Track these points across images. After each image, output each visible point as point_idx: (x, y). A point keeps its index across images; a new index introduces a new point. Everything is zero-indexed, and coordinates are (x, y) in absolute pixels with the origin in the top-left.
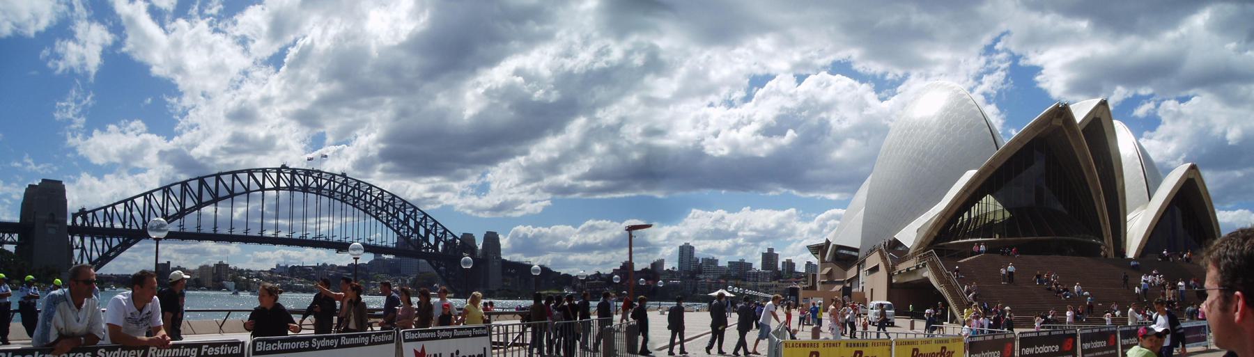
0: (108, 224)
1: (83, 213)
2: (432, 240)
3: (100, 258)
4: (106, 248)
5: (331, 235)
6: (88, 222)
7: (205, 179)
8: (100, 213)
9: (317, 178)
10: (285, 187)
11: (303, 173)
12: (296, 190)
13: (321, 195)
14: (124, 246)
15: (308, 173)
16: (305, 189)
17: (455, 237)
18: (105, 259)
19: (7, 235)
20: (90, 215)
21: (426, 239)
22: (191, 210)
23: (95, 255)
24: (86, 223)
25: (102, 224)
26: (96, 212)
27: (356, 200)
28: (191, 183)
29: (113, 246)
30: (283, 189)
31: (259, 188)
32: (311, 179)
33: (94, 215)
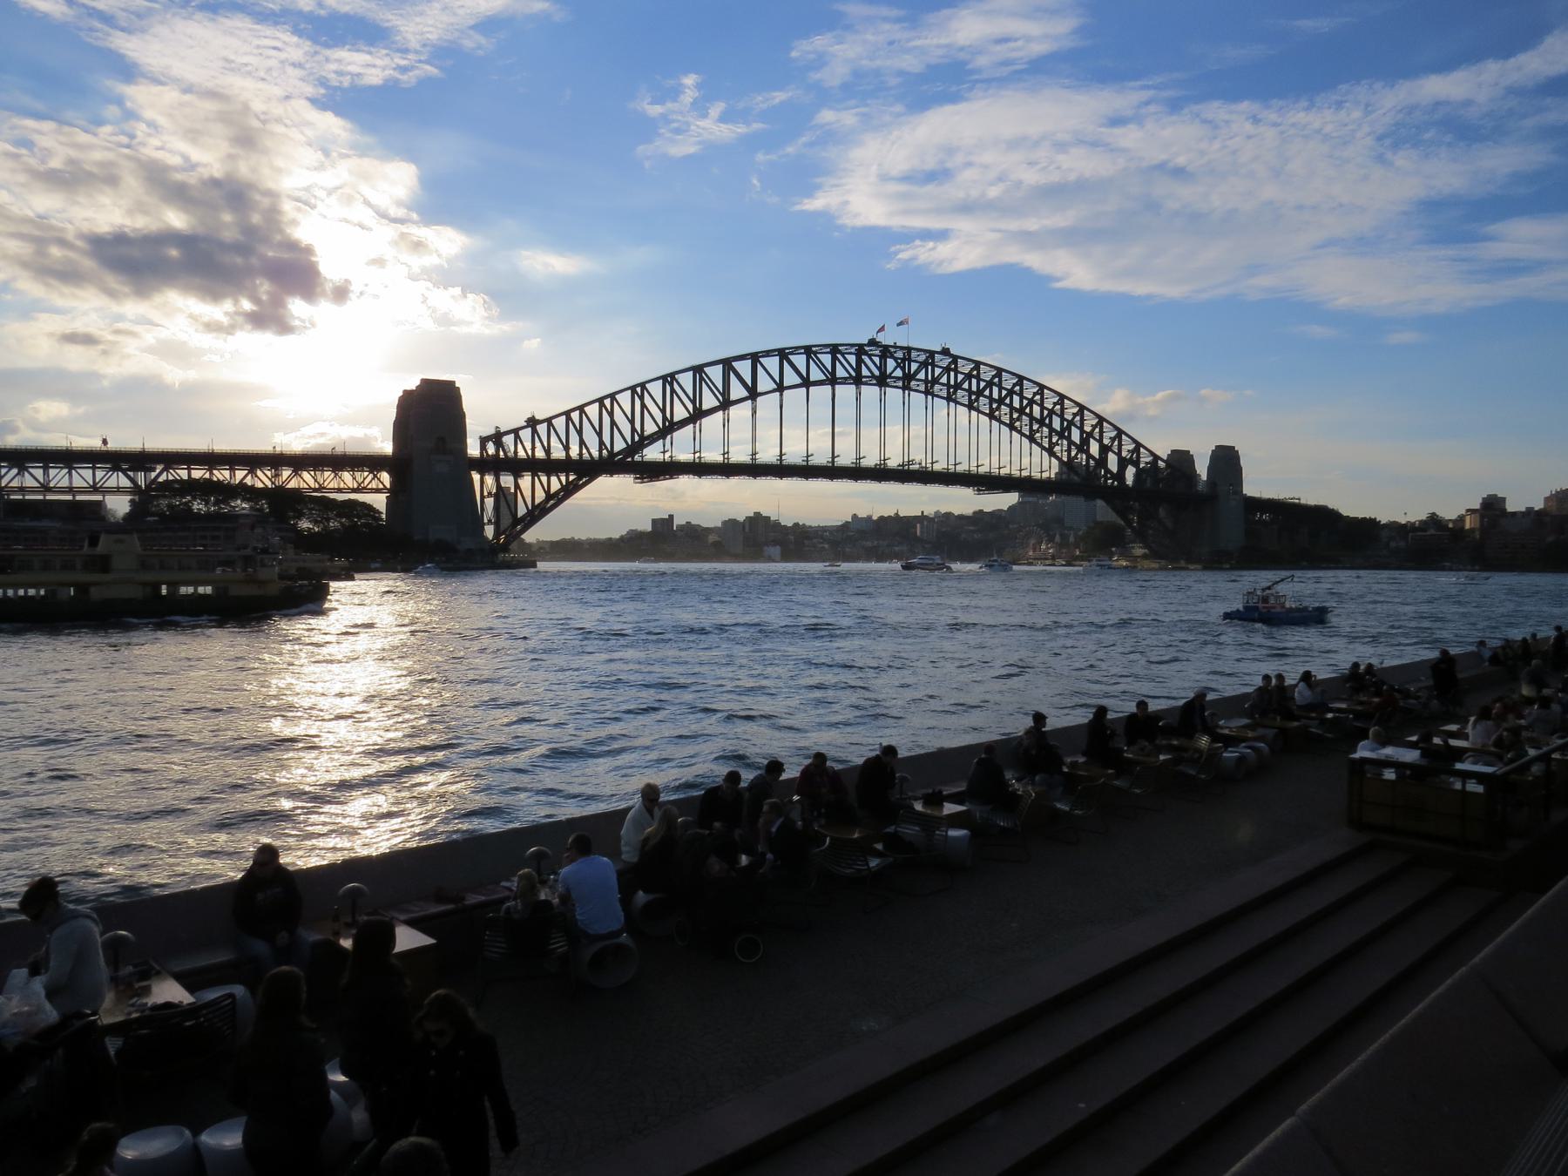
0: (540, 454)
1: (497, 437)
2: (1113, 462)
4: (540, 496)
5: (929, 461)
6: (504, 450)
8: (526, 434)
9: (903, 360)
10: (845, 378)
11: (877, 352)
12: (866, 384)
13: (910, 389)
14: (569, 490)
15: (886, 352)
16: (882, 381)
17: (1156, 458)
18: (538, 513)
19: (371, 476)
20: (508, 440)
21: (1103, 461)
23: (522, 511)
24: (501, 453)
25: (530, 453)
26: (520, 432)
27: (973, 397)
29: (553, 490)
30: (844, 381)
31: (798, 381)
32: (891, 364)
33: (517, 437)
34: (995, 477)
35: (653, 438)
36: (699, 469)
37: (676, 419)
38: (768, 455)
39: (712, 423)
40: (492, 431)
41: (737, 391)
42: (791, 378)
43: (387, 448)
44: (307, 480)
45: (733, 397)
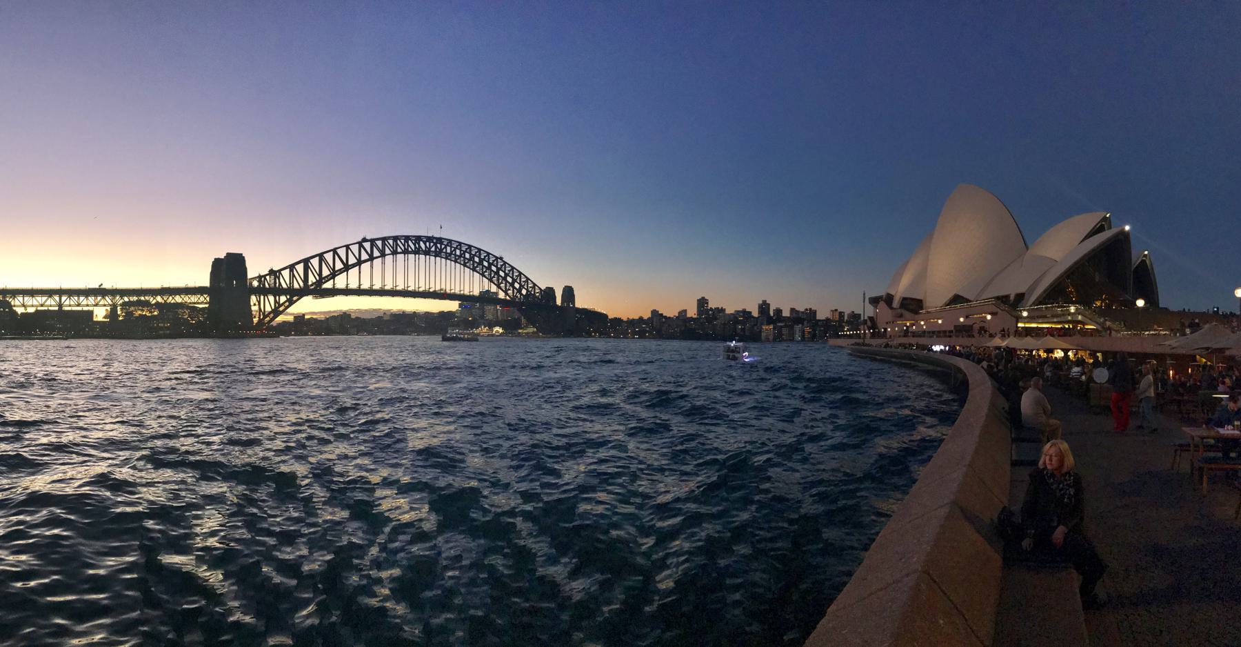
1: (260, 278)
2: (524, 292)
3: (273, 311)
7: (350, 246)
14: (291, 302)
15: (430, 239)
18: (276, 312)
21: (519, 291)
22: (341, 271)
28: (338, 251)
29: (281, 302)
30: (410, 253)
34: (468, 296)
35: (328, 278)
36: (347, 292)
37: (336, 269)
38: (377, 286)
39: (354, 272)
40: (257, 275)
41: (364, 256)
42: (387, 251)
43: (208, 284)
44: (178, 299)
45: (363, 259)
